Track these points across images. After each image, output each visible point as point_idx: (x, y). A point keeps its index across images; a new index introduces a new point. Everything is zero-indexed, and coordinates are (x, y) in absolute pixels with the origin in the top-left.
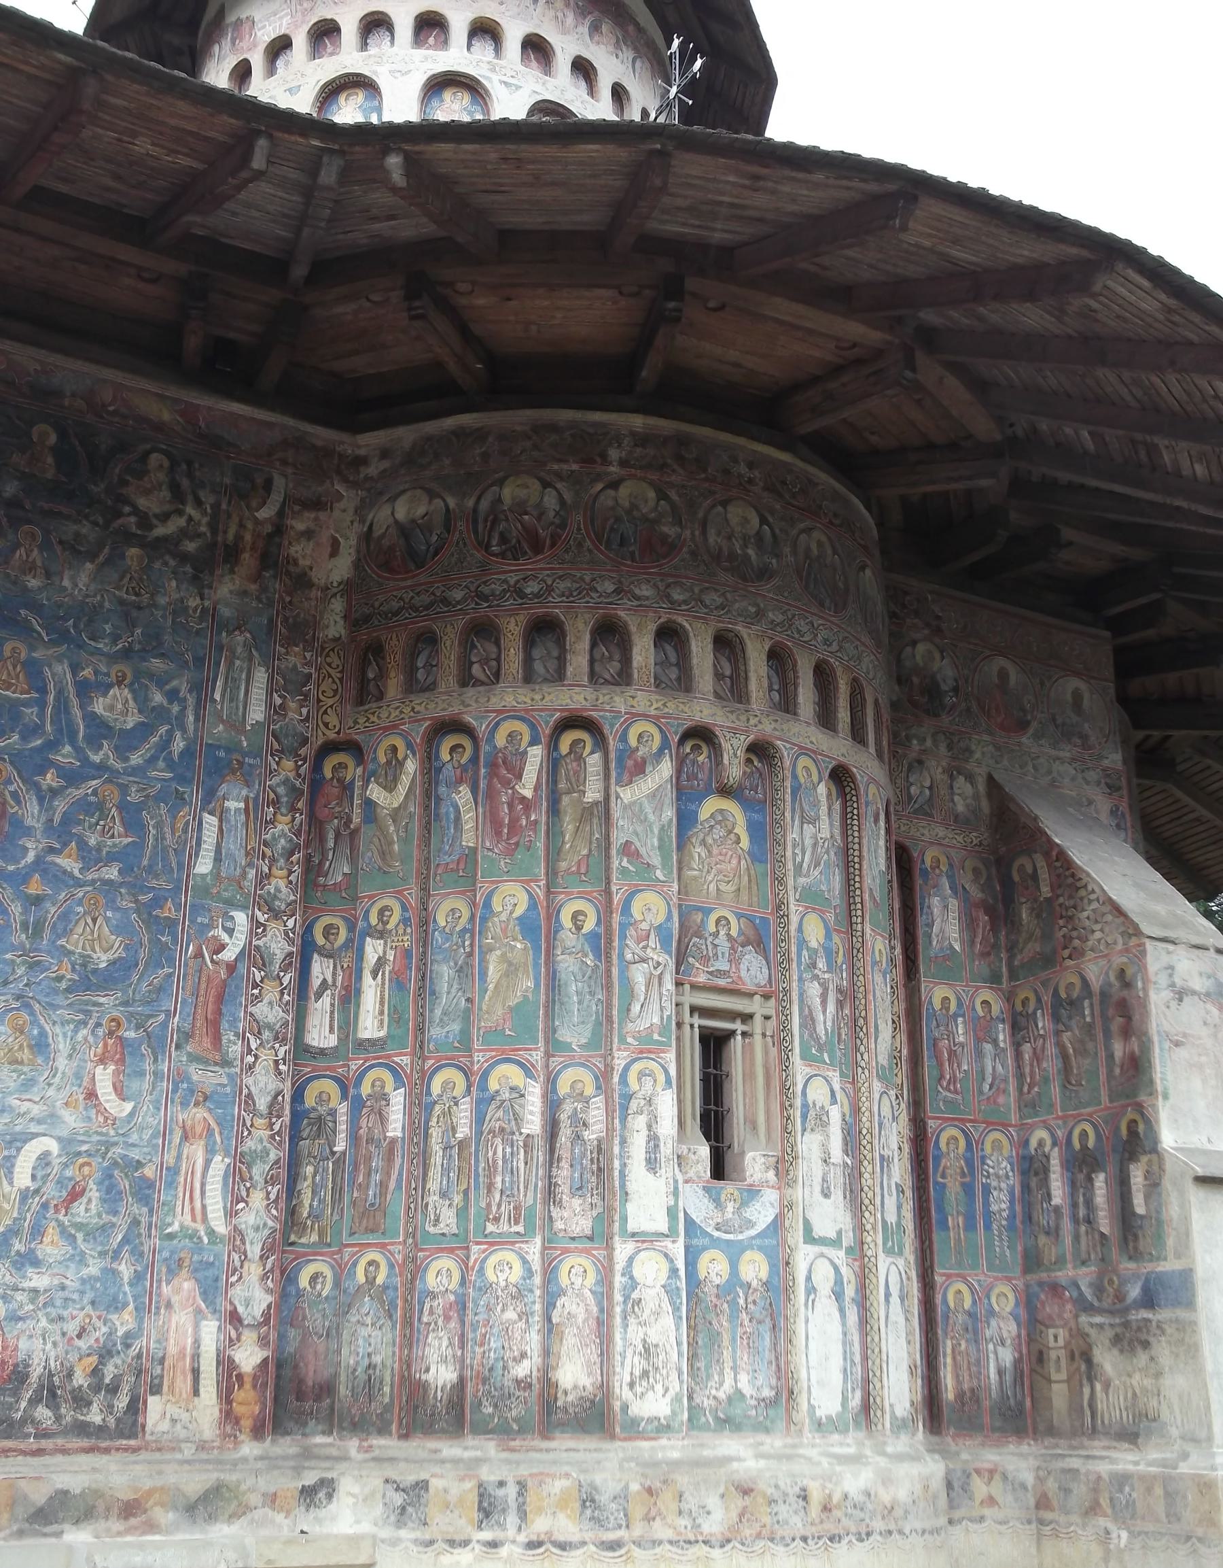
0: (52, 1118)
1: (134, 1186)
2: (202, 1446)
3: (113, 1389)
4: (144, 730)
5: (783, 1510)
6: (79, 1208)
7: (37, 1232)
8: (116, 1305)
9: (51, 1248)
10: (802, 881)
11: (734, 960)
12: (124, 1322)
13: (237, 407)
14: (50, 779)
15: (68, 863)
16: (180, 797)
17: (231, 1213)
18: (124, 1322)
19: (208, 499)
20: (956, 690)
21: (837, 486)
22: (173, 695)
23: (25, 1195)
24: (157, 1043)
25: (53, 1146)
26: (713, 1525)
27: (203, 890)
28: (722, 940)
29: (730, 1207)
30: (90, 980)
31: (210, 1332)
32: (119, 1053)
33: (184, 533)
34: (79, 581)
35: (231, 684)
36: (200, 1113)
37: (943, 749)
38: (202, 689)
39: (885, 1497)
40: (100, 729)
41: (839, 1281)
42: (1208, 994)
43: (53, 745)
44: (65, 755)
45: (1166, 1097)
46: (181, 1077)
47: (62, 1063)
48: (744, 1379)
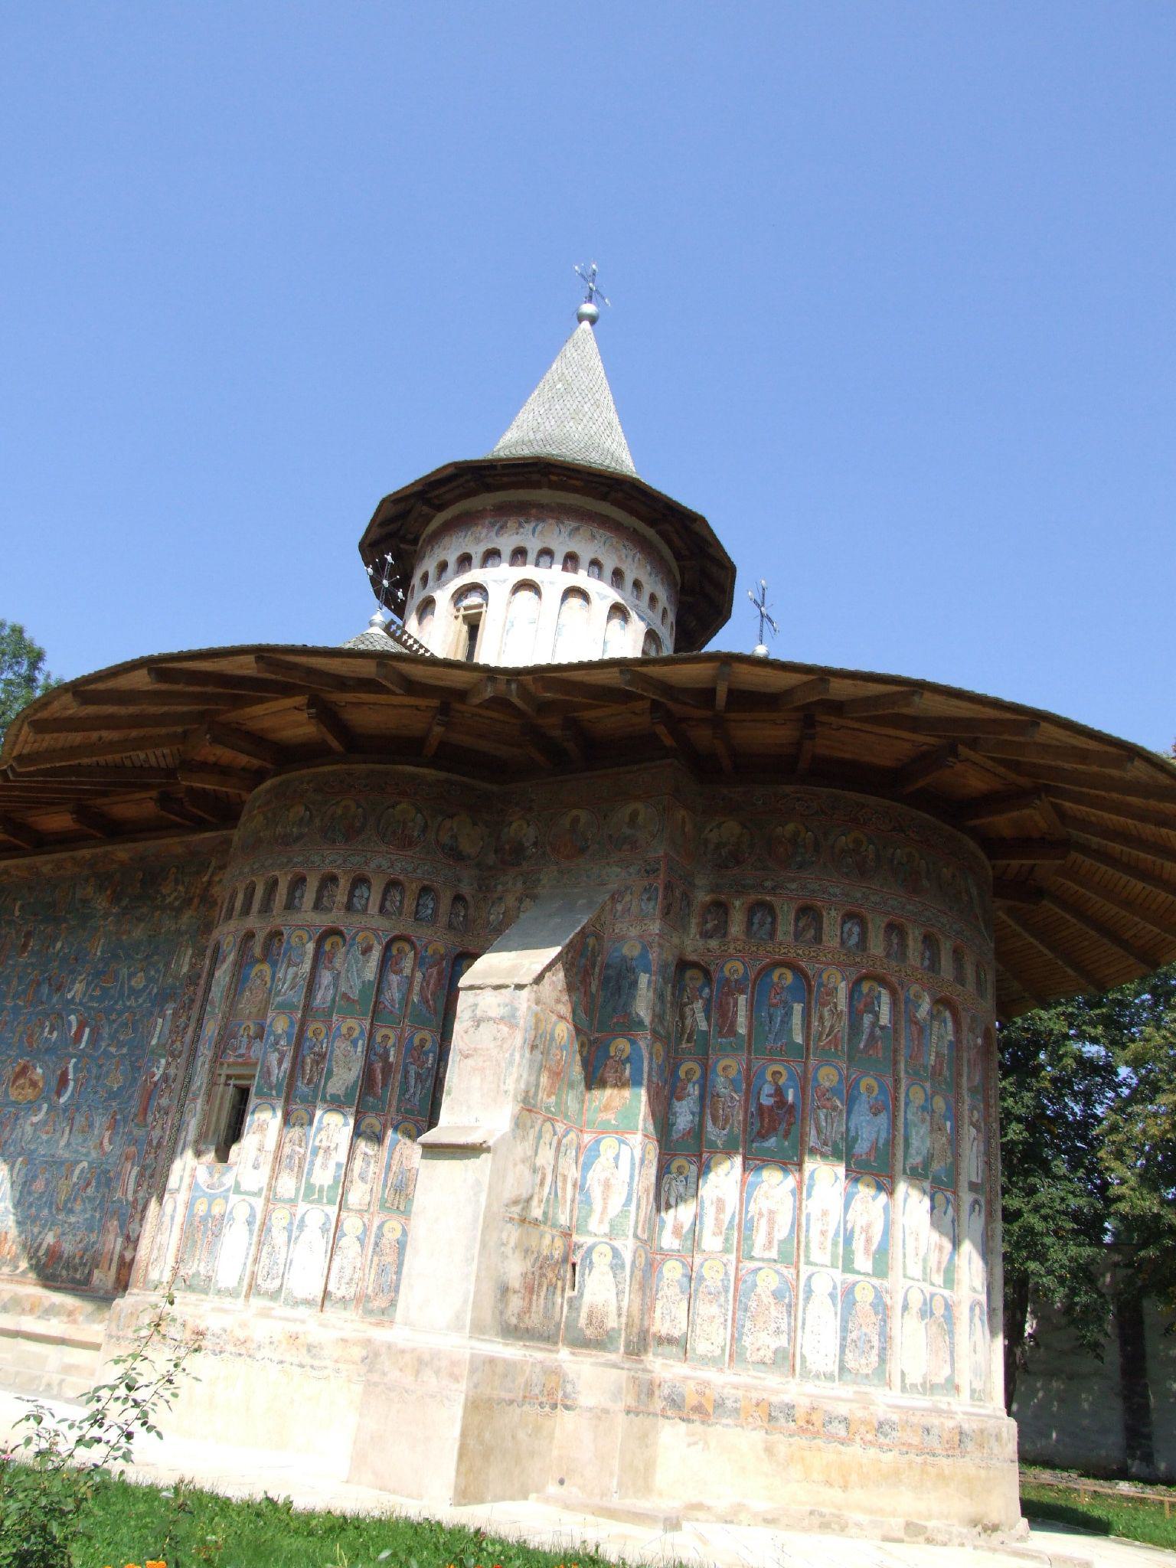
0: (87, 1154)
2: (106, 1292)
3: (85, 1265)
4: (146, 987)
6: (89, 1190)
7: (75, 1200)
8: (92, 1231)
9: (78, 1207)
10: (279, 999)
11: (249, 1048)
12: (93, 1237)
13: (207, 835)
14: (113, 1017)
15: (113, 1050)
16: (151, 1014)
17: (136, 1192)
18: (93, 1237)
19: (186, 880)
20: (535, 844)
21: (371, 766)
22: (158, 971)
23: (75, 1184)
24: (125, 1120)
25: (85, 1164)
27: (153, 1052)
28: (245, 1039)
29: (217, 1176)
30: (112, 1095)
31: (120, 1240)
32: (114, 1126)
33: (176, 899)
34: (138, 933)
35: (179, 957)
36: (133, 1149)
37: (519, 885)
38: (167, 965)
39: (241, 1334)
40: (132, 990)
41: (253, 1215)
42: (502, 1018)
43: (116, 1002)
45: (449, 1094)
46: (131, 1132)
47: (96, 1132)
48: (203, 1264)
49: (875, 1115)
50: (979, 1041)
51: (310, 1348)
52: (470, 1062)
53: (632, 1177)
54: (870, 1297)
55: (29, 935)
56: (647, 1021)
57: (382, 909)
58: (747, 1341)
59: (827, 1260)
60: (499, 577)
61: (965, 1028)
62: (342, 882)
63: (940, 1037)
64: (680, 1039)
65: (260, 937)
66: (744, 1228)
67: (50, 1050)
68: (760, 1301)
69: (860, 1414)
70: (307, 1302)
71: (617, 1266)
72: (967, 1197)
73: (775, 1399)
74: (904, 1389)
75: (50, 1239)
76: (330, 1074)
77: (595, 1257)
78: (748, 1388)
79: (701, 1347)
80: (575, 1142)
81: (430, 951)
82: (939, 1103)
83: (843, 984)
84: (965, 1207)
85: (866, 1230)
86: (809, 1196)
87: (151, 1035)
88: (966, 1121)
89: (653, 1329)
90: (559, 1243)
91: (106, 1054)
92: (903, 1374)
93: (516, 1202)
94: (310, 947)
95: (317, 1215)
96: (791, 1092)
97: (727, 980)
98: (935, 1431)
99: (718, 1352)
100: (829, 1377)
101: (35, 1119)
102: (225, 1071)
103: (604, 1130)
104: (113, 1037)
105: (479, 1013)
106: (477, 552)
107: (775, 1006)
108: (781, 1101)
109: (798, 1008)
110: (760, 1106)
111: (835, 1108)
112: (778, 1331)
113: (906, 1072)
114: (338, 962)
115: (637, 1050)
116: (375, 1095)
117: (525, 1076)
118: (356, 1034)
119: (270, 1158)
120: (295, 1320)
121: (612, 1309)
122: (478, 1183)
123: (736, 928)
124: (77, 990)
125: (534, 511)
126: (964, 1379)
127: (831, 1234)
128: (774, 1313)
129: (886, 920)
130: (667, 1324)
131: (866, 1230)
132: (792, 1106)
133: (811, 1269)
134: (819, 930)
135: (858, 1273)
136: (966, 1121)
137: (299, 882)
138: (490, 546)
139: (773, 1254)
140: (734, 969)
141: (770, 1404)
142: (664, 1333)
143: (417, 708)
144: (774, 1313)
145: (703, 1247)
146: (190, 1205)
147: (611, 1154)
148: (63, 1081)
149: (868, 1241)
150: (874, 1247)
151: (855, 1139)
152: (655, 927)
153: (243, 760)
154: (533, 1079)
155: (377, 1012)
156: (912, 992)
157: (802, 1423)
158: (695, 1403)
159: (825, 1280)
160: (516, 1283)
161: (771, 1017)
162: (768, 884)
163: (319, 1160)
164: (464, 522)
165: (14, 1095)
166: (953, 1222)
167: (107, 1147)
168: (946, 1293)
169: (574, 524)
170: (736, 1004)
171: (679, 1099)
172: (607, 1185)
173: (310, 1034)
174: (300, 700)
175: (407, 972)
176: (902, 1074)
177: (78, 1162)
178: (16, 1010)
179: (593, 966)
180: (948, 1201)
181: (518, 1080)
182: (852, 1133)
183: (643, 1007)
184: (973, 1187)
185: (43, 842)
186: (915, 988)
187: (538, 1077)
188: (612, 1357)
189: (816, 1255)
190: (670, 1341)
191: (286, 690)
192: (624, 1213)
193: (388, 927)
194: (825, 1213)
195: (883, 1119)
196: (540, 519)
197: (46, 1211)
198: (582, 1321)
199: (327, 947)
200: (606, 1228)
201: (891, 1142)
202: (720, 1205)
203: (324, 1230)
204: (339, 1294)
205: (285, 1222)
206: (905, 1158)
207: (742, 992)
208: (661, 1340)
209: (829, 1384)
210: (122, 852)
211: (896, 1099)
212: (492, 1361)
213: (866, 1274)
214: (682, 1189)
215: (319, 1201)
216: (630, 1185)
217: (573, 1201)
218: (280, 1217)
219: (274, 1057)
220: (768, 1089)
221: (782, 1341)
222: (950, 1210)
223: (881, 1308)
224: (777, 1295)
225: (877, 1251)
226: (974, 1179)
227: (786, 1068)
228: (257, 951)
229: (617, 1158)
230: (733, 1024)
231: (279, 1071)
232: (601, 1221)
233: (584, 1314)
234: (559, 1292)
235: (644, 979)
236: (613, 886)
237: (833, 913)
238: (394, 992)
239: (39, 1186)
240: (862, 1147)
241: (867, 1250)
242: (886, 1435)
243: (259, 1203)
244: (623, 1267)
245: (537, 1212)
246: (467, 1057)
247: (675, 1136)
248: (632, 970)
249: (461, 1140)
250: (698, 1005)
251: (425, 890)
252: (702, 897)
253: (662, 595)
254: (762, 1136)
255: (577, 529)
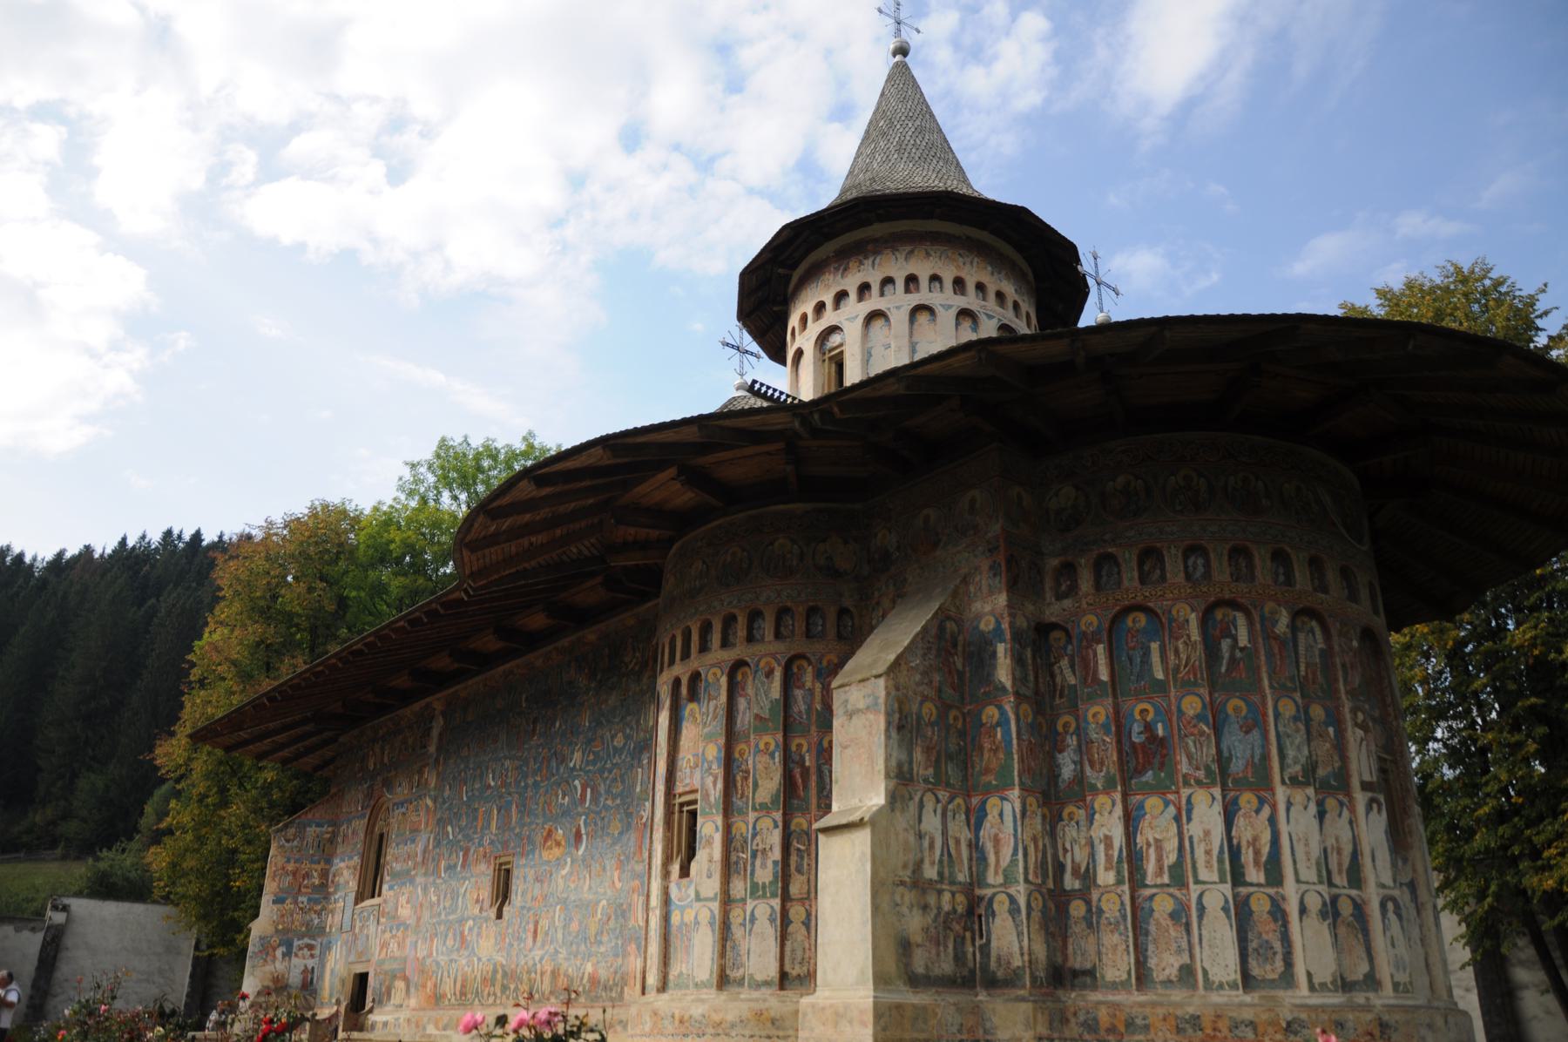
1: (621, 911)
5: (666, 1022)
8: (616, 955)
9: (605, 939)
11: (691, 777)
12: (620, 961)
15: (609, 802)
25: (604, 902)
26: (647, 1028)
32: (621, 865)
39: (716, 1018)
40: (615, 749)
41: (713, 916)
44: (608, 765)
49: (1247, 733)
50: (1355, 644)
51: (773, 1021)
52: (849, 751)
53: (1015, 830)
54: (1267, 906)
55: (535, 721)
56: (1008, 684)
57: (778, 635)
58: (1152, 963)
59: (1215, 878)
60: (851, 315)
61: (1334, 632)
62: (740, 619)
63: (1309, 648)
64: (1054, 697)
65: (684, 682)
66: (1133, 859)
67: (566, 813)
68: (1158, 924)
69: (1264, 1017)
70: (767, 983)
71: (1014, 910)
72: (1361, 798)
73: (1179, 1013)
74: (1312, 988)
75: (589, 968)
76: (756, 785)
77: (995, 906)
78: (1154, 1004)
79: (1111, 974)
80: (963, 807)
81: (825, 663)
82: (1317, 712)
83: (1193, 615)
84: (1361, 809)
85: (1255, 840)
86: (1189, 819)
87: (634, 786)
88: (1349, 724)
89: (1069, 964)
90: (960, 898)
91: (606, 808)
92: (1309, 975)
93: (905, 866)
94: (724, 680)
95: (765, 909)
96: (1160, 726)
97: (1084, 633)
98: (1350, 1024)
99: (1125, 976)
100: (1233, 986)
101: (564, 872)
102: (678, 801)
103: (988, 791)
104: (608, 791)
105: (850, 707)
106: (828, 299)
107: (1133, 648)
108: (1152, 737)
109: (1155, 646)
110: (1133, 745)
111: (1202, 733)
112: (1179, 951)
113: (1271, 686)
114: (750, 690)
115: (1003, 713)
116: (798, 797)
117: (895, 754)
118: (772, 747)
119: (717, 869)
120: (757, 1000)
121: (1016, 948)
122: (863, 854)
123: (1086, 584)
124: (577, 756)
125: (870, 247)
126: (1385, 972)
127: (1215, 852)
128: (1173, 934)
129: (1228, 547)
130: (1079, 959)
131: (1255, 840)
132: (1163, 739)
133: (1199, 888)
134: (1163, 570)
135: (1252, 885)
136: (1349, 724)
137: (706, 629)
138: (839, 289)
139: (1166, 879)
140: (1090, 622)
141: (1177, 1018)
142: (1077, 966)
143: (768, 453)
144: (1173, 934)
145: (1100, 881)
146: (666, 918)
147: (996, 812)
148: (578, 836)
149: (1257, 853)
150: (1264, 859)
151: (1230, 759)
152: (1002, 599)
153: (654, 534)
154: (904, 757)
155: (787, 729)
156: (1266, 609)
157: (1209, 1031)
158: (1107, 1025)
159: (1217, 895)
160: (917, 938)
161: (1130, 659)
162: (1107, 537)
163: (758, 862)
164: (814, 273)
165: (545, 855)
166: (1351, 822)
167: (618, 885)
168: (1354, 893)
169: (908, 248)
170: (1095, 655)
171: (1061, 751)
172: (997, 841)
173: (737, 755)
174: (672, 471)
175: (808, 685)
176: (1268, 691)
177: (597, 903)
178: (536, 784)
179: (955, 645)
180: (1341, 804)
181: (887, 760)
182: (1226, 754)
183: (1004, 673)
184: (1365, 786)
185: (534, 640)
186: (1269, 606)
187: (910, 754)
188: (1022, 992)
189: (1203, 874)
190: (1086, 973)
191: (660, 466)
192: (1014, 862)
193: (783, 649)
194: (1207, 833)
195: (1256, 734)
196: (876, 253)
197: (583, 947)
198: (993, 965)
199: (739, 677)
200: (1000, 880)
201: (1266, 757)
202: (1108, 841)
203: (772, 920)
204: (794, 973)
205: (740, 920)
206: (1282, 769)
207: (1099, 642)
208: (1076, 974)
209: (1234, 993)
210: (590, 635)
211: (1265, 715)
212: (899, 1007)
213: (1259, 885)
214: (1075, 834)
215: (764, 896)
216: (1015, 836)
217: (970, 859)
218: (736, 915)
219: (709, 780)
220: (1136, 728)
221: (1186, 959)
222: (1346, 813)
223: (1278, 912)
224: (1174, 916)
225: (1266, 863)
226: (1367, 778)
227: (1153, 705)
228: (684, 691)
229: (1001, 815)
230: (1096, 671)
231: (716, 792)
232: (996, 873)
233: (993, 959)
234: (968, 941)
235: (1001, 648)
236: (964, 571)
237: (1173, 551)
238: (800, 706)
239: (574, 926)
240: (1237, 767)
241: (1256, 863)
242: (1296, 1033)
243: (715, 906)
244: (1019, 911)
245: (930, 873)
246: (846, 747)
247: (1062, 786)
248: (991, 643)
249: (844, 821)
250: (1065, 663)
251: (812, 611)
252: (1055, 562)
253: (1009, 289)
254: (1140, 772)
255: (912, 252)
